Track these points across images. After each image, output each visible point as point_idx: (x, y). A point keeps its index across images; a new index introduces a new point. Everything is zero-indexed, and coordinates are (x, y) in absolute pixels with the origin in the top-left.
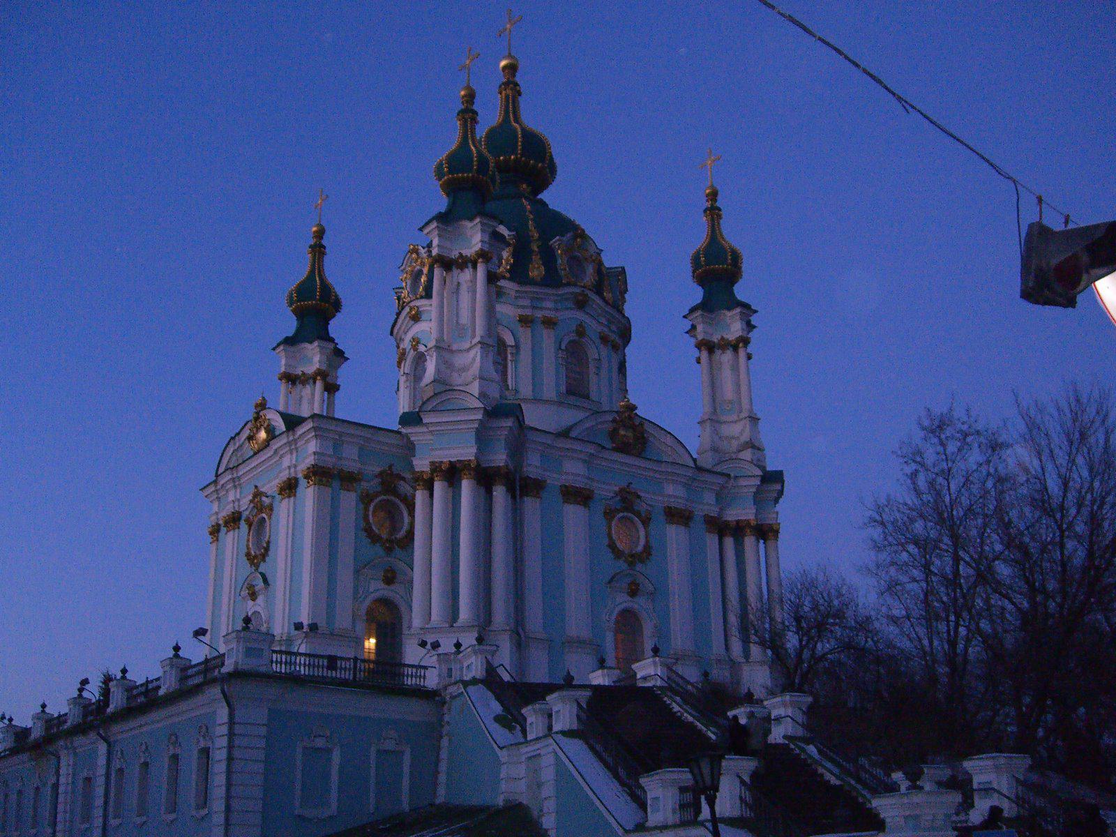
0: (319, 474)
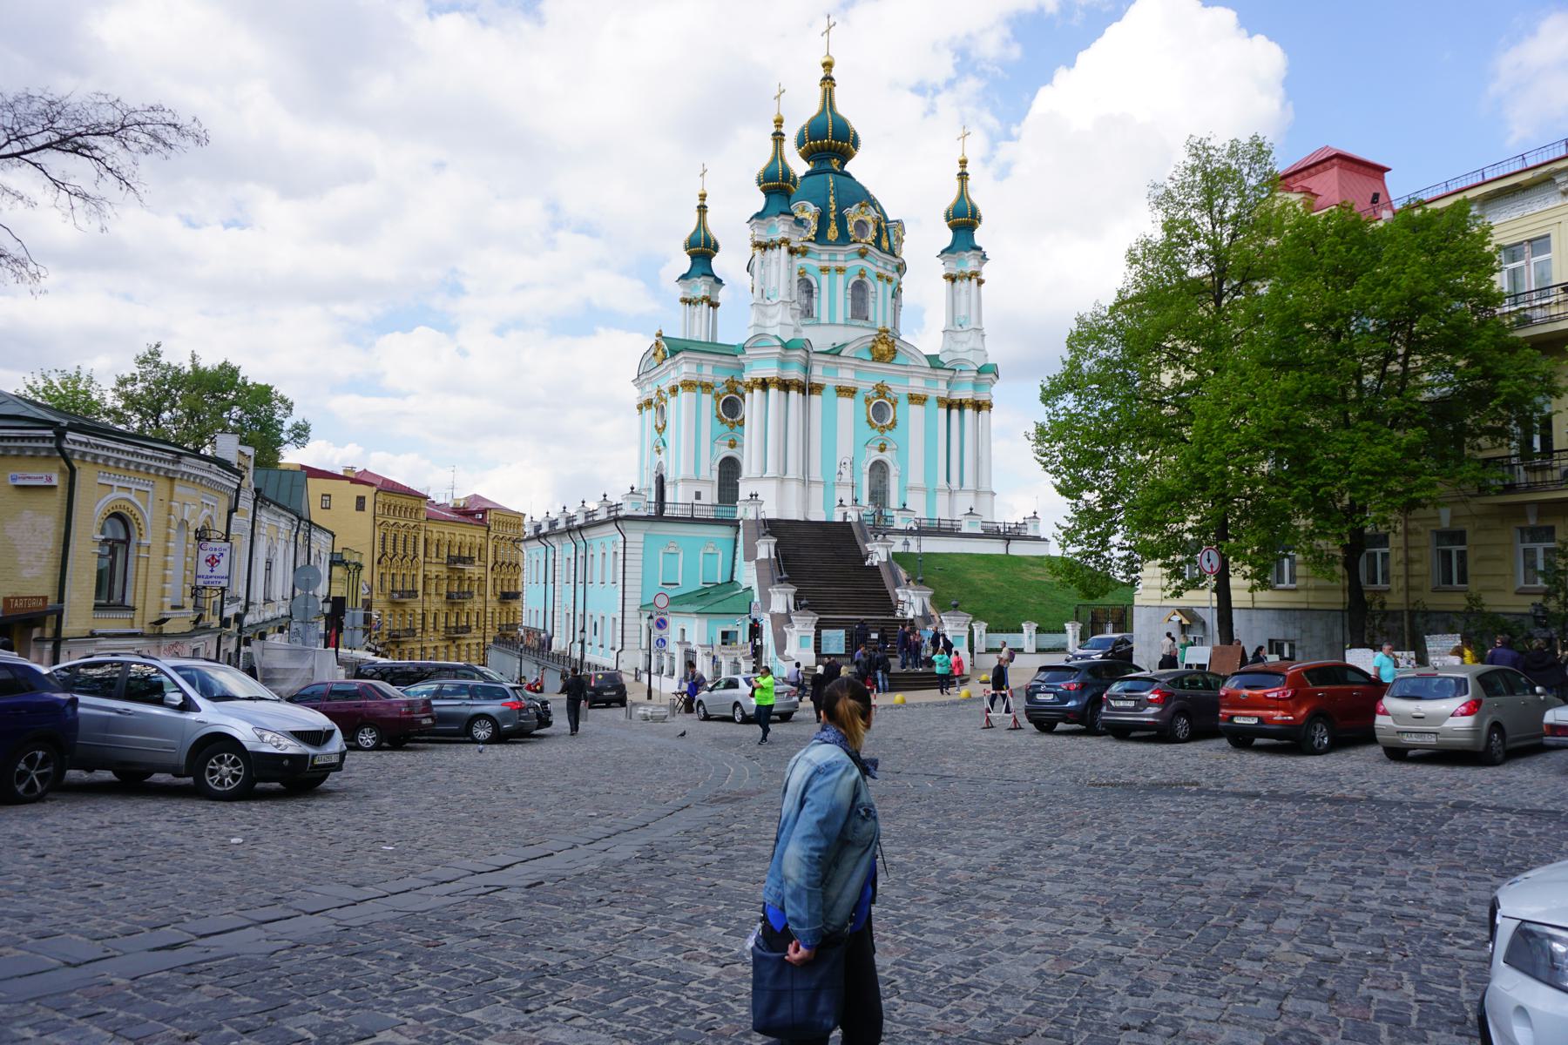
0: (688, 385)
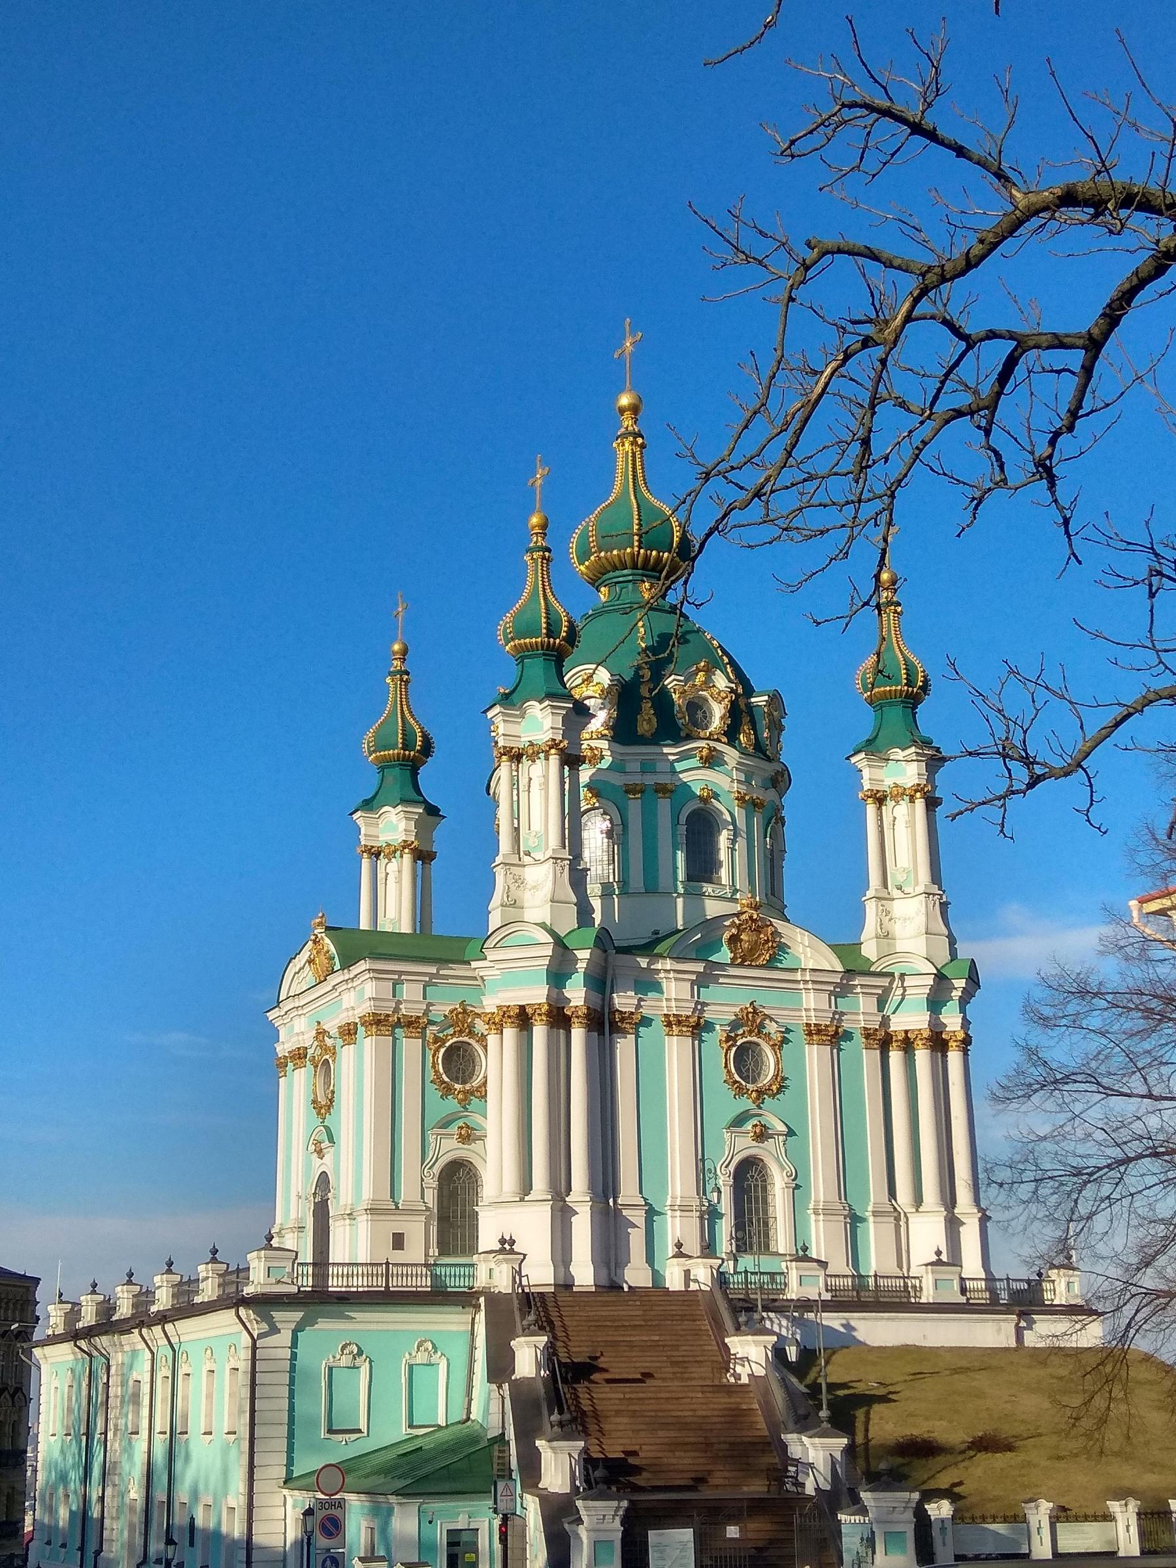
0: (377, 1022)
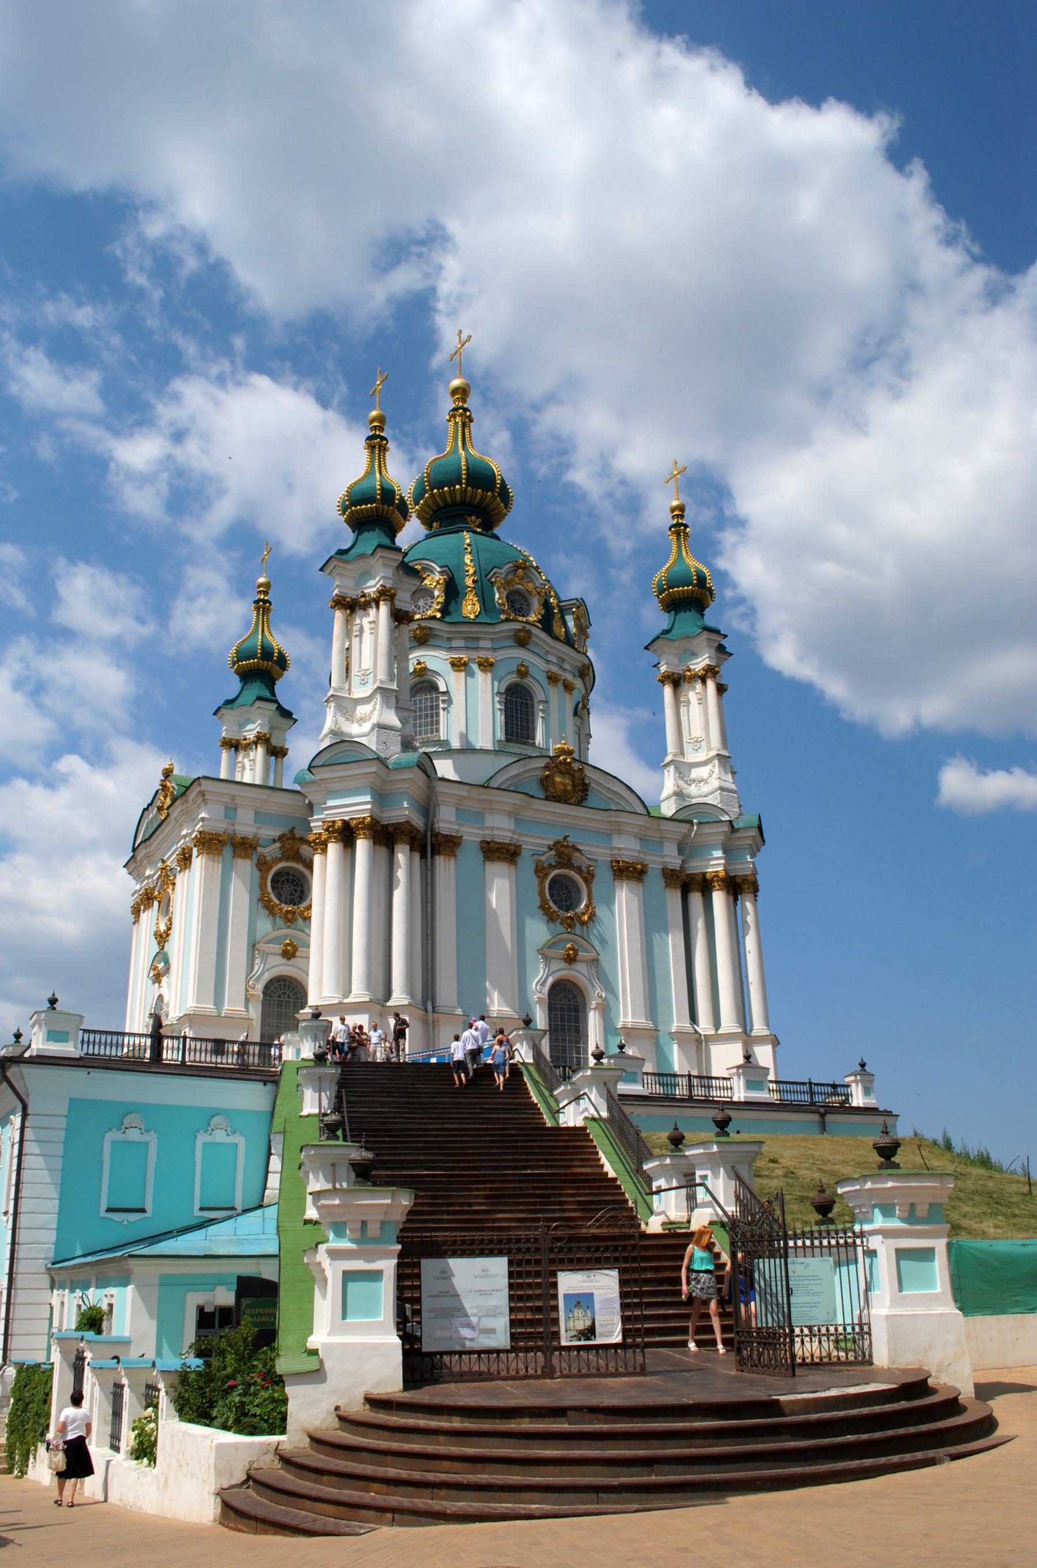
0: (209, 843)
